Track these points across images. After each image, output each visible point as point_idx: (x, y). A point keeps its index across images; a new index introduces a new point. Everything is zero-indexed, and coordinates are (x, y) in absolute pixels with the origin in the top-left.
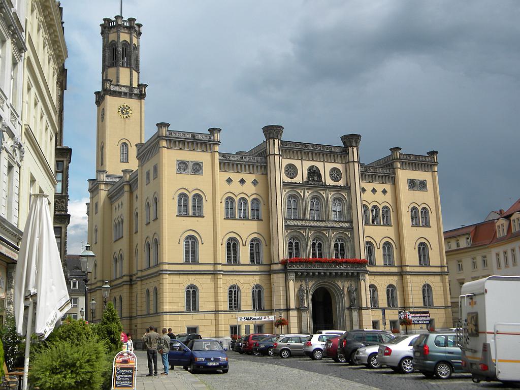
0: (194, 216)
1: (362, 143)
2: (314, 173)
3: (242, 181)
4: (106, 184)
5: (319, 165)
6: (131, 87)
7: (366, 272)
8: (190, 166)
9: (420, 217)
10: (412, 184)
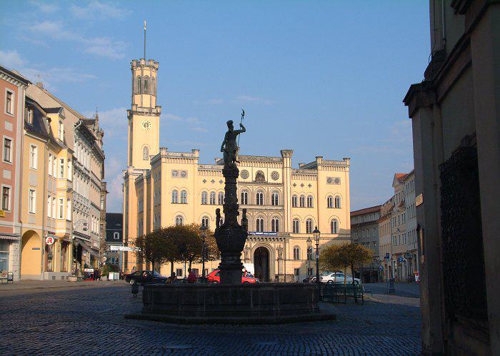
0: (182, 203)
1: (293, 155)
2: (260, 176)
3: (213, 181)
4: (133, 174)
5: (264, 170)
6: (151, 109)
7: (292, 238)
8: (180, 173)
9: (333, 203)
10: (329, 180)
